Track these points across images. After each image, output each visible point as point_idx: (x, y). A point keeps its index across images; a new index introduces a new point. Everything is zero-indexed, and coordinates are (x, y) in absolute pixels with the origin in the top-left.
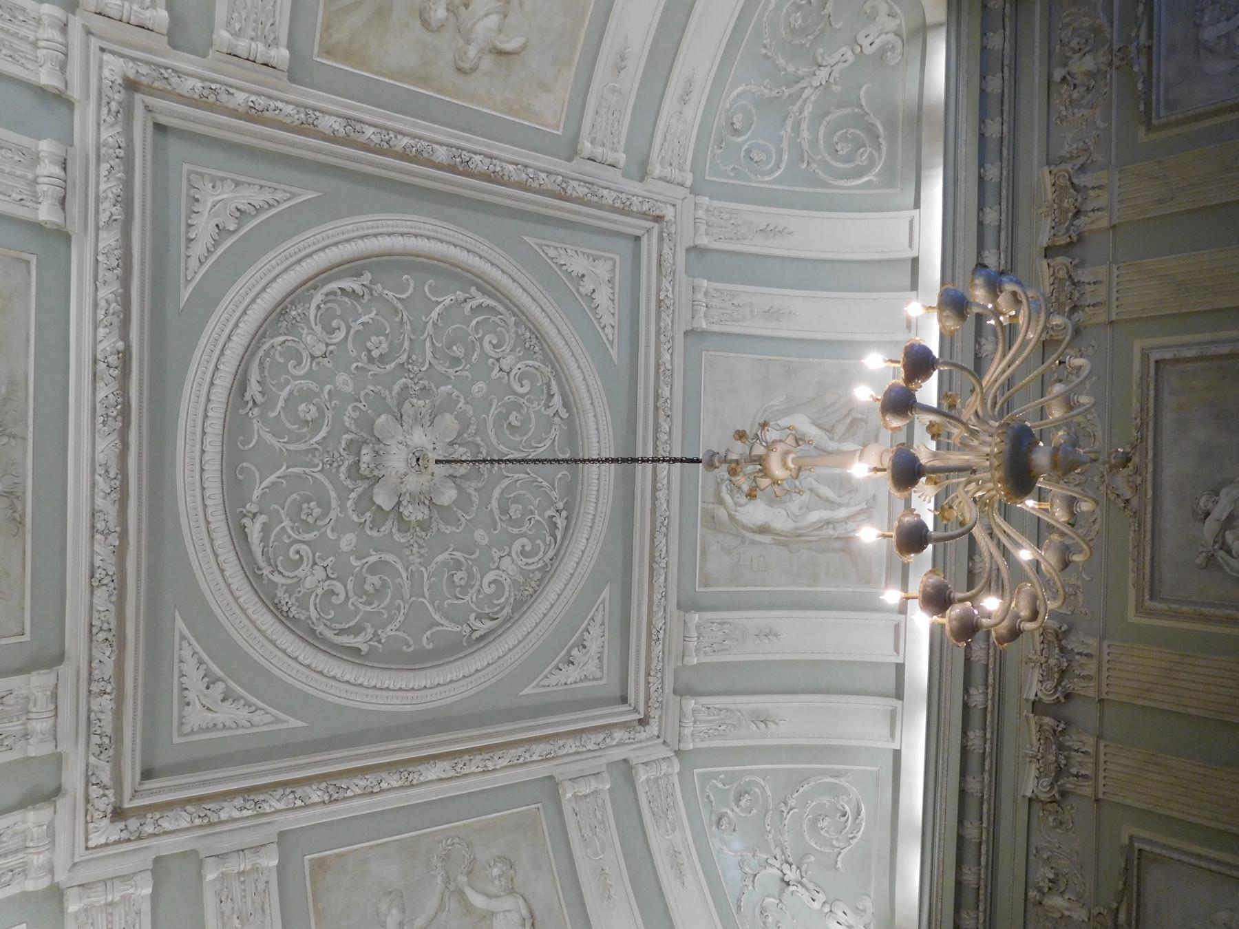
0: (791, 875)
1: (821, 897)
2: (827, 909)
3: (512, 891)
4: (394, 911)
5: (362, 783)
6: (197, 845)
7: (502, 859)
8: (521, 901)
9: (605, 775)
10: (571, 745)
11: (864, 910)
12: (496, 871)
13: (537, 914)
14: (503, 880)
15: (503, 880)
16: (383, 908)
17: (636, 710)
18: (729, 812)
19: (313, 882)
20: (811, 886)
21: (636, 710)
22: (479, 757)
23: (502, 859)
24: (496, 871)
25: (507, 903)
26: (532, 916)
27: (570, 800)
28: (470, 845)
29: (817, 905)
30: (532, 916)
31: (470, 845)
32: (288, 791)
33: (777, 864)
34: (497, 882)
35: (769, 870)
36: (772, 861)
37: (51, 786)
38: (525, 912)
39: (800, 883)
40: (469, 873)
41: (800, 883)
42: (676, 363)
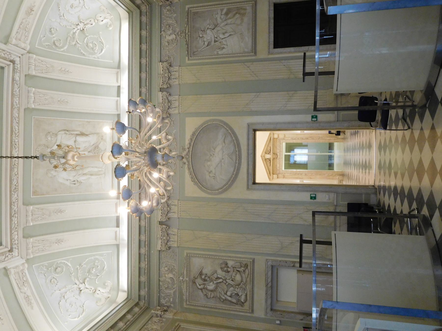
0: (81, 26)
1: (93, 21)
2: (96, 21)
3: (56, 135)
4: (52, 172)
5: (15, 180)
6: (22, 227)
7: (46, 135)
8: (60, 133)
9: (29, 89)
10: (16, 100)
11: (104, 10)
12: (49, 139)
13: (65, 129)
14: (53, 137)
15: (53, 137)
16: (50, 175)
17: (9, 65)
18: (55, 39)
19: (38, 195)
20: (88, 21)
21: (9, 65)
22: (14, 138)
23: (46, 135)
24: (49, 139)
25: (59, 137)
26: (65, 130)
27: (34, 105)
28: (39, 145)
29: (94, 24)
30: (65, 130)
31: (39, 145)
32: (13, 204)
33: (76, 29)
34: (53, 139)
35: (77, 34)
36: (75, 31)
37: (3, 271)
38: (63, 132)
39: (85, 25)
40: (48, 148)
41: (85, 25)
42: (19, 181)
